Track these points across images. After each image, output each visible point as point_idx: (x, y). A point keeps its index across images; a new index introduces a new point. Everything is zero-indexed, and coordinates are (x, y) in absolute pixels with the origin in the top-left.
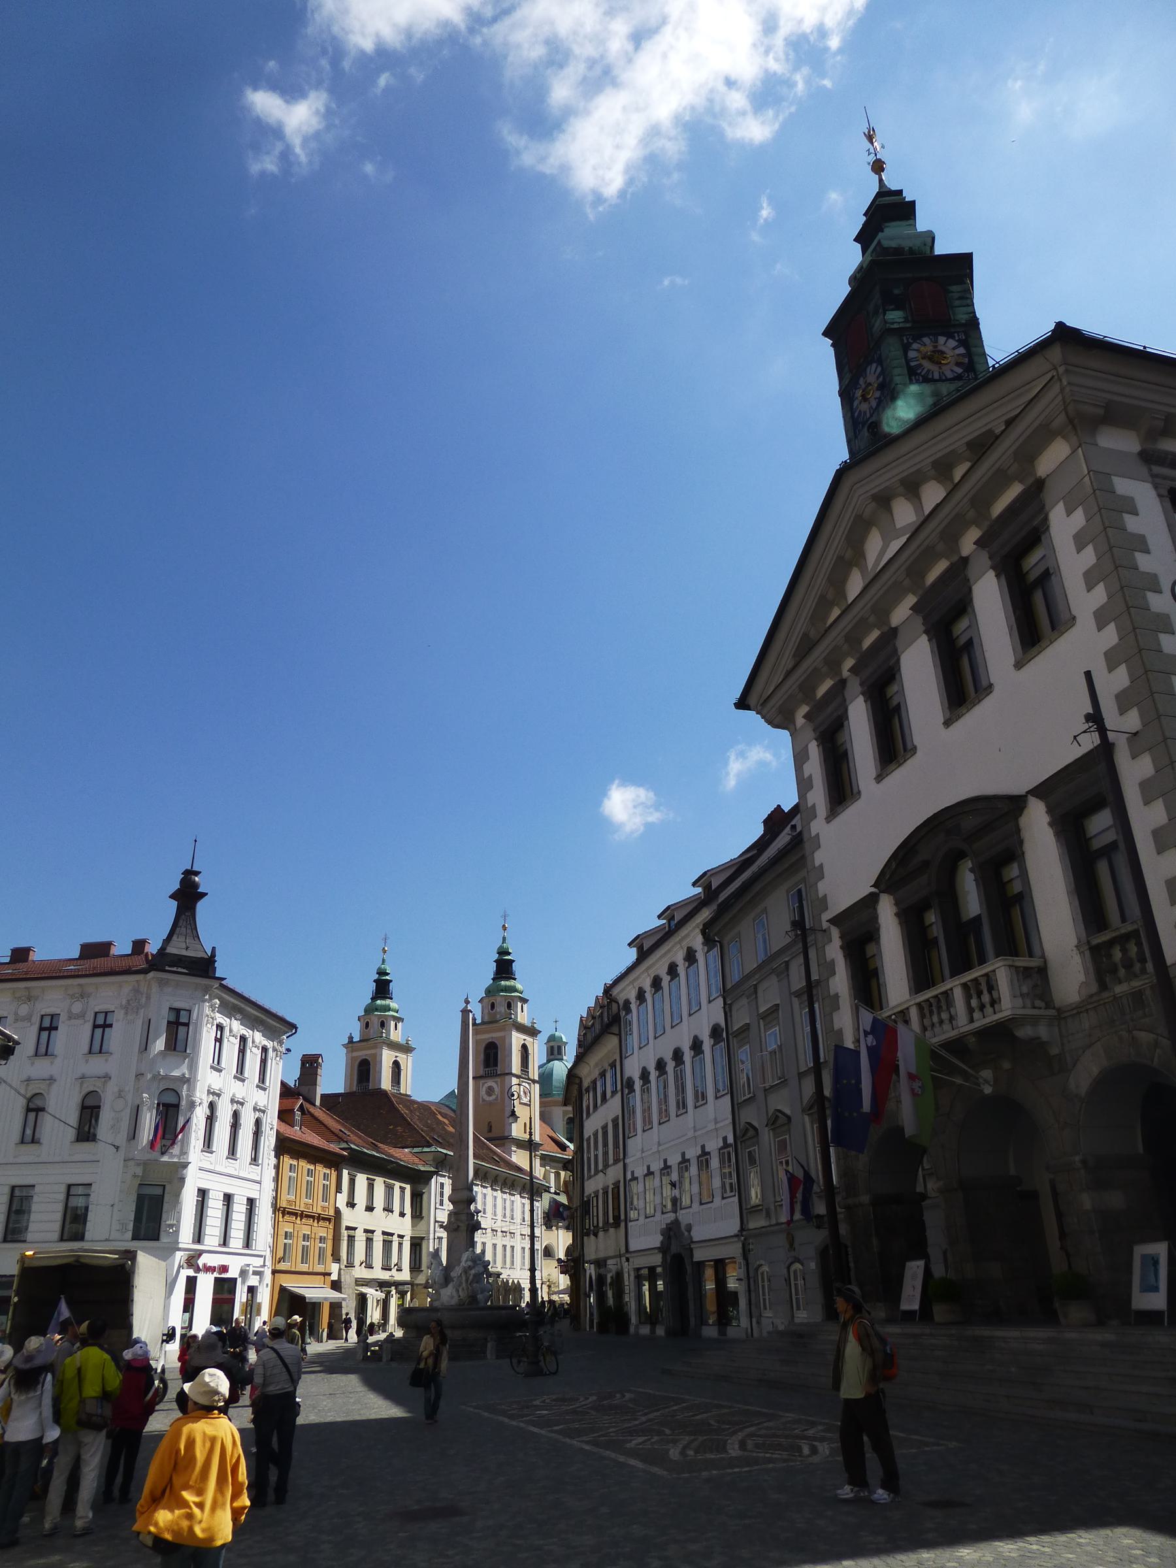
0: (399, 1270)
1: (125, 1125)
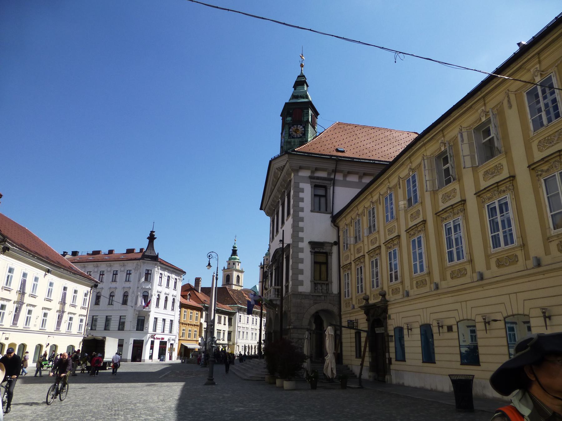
0: (223, 340)
1: (134, 301)
